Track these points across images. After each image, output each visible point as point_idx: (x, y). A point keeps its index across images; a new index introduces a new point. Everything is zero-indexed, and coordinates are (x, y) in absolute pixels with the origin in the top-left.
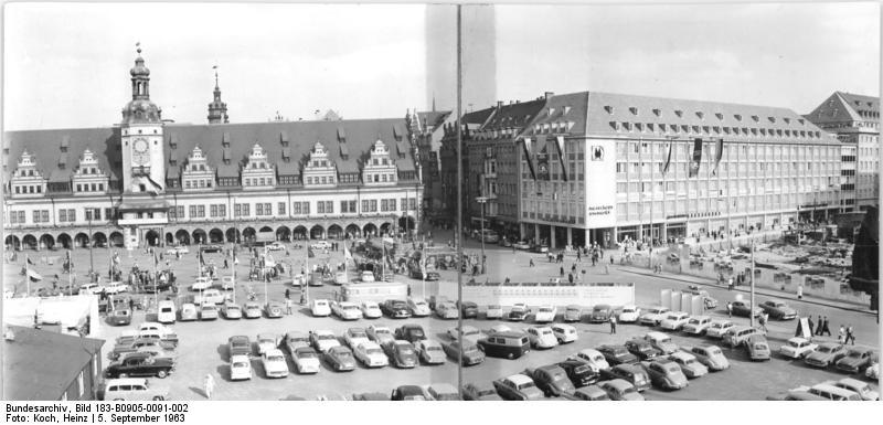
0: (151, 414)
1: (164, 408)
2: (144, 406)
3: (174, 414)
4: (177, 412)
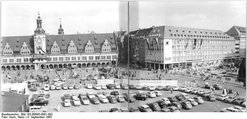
0: (42, 116)
1: (46, 114)
2: (40, 114)
3: (49, 116)
4: (50, 115)
